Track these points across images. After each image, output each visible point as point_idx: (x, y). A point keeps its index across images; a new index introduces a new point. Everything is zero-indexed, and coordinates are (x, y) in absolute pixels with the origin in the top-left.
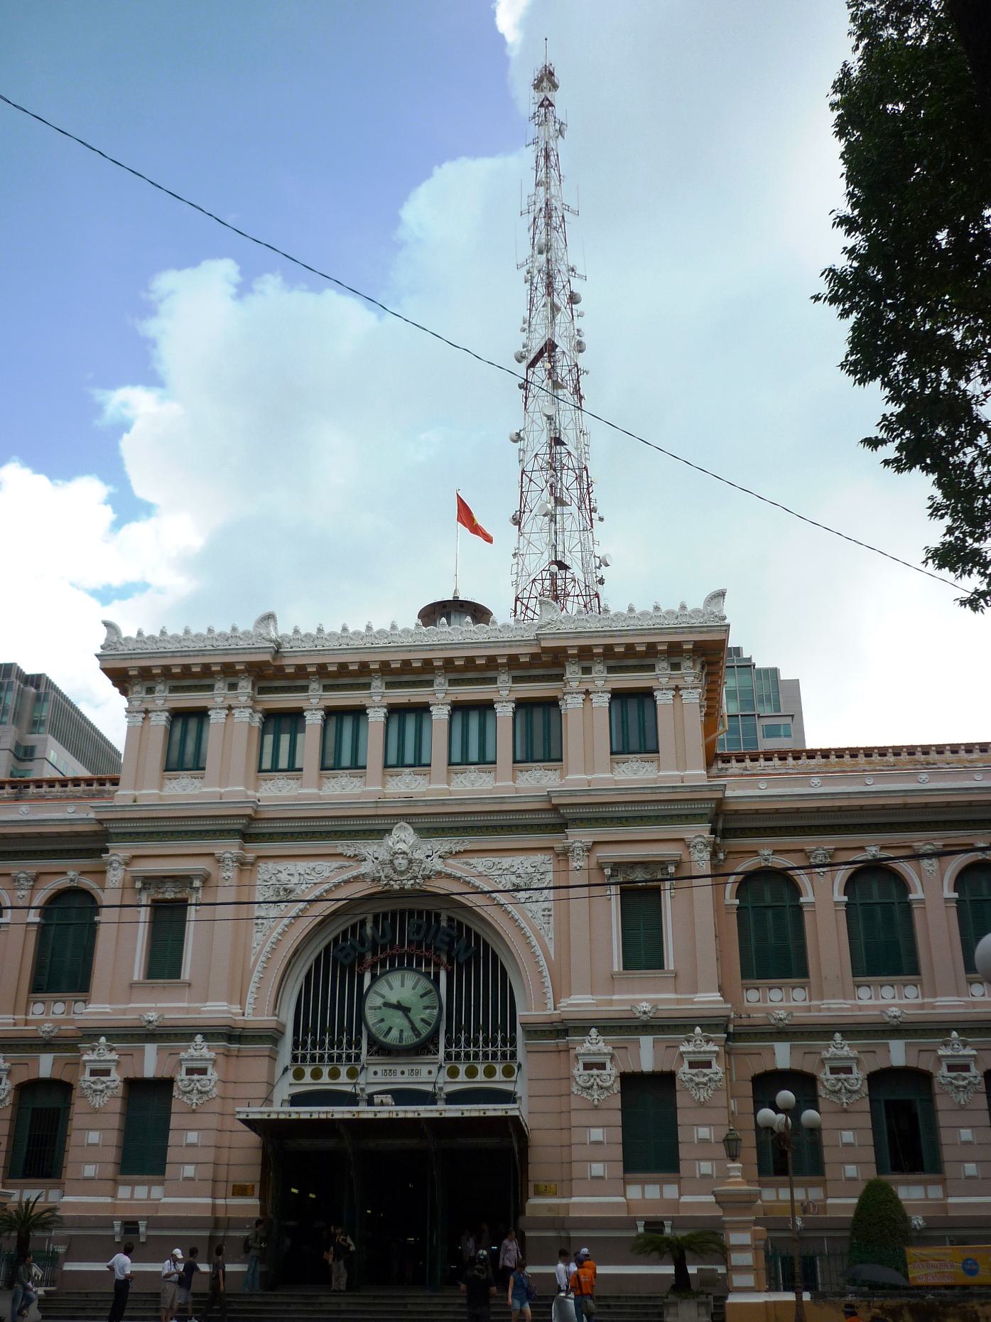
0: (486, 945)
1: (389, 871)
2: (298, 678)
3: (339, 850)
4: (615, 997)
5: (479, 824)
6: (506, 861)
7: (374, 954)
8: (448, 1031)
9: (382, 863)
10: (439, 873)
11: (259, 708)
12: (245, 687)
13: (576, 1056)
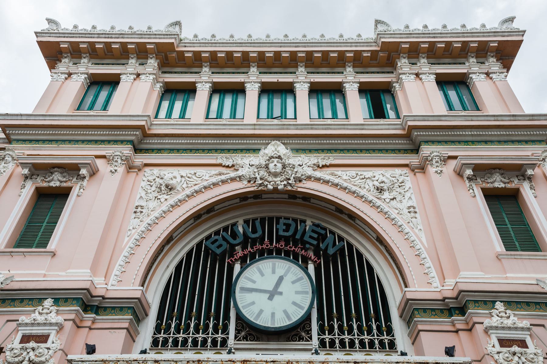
0: (350, 246)
1: (263, 173)
2: (196, 61)
3: (219, 161)
4: (508, 275)
5: (341, 147)
6: (368, 173)
7: (244, 248)
8: (320, 317)
9: (259, 167)
10: (309, 178)
11: (161, 80)
12: (152, 63)
13: (486, 331)
